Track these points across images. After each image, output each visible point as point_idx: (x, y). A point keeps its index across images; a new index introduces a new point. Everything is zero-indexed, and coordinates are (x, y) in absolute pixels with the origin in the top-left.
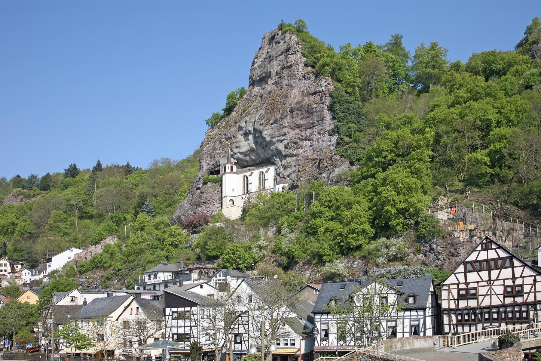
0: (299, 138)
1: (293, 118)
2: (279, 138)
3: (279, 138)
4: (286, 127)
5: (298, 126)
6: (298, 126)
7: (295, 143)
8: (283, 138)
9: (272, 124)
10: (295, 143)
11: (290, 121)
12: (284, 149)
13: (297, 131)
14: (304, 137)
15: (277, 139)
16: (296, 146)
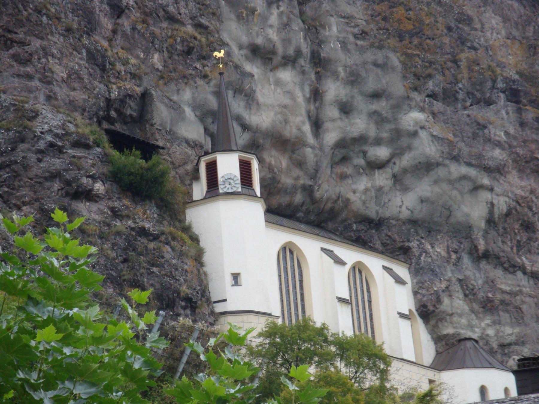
1: (522, 124)
2: (472, 172)
4: (498, 144)
9: (432, 96)
11: (512, 131)
15: (464, 170)
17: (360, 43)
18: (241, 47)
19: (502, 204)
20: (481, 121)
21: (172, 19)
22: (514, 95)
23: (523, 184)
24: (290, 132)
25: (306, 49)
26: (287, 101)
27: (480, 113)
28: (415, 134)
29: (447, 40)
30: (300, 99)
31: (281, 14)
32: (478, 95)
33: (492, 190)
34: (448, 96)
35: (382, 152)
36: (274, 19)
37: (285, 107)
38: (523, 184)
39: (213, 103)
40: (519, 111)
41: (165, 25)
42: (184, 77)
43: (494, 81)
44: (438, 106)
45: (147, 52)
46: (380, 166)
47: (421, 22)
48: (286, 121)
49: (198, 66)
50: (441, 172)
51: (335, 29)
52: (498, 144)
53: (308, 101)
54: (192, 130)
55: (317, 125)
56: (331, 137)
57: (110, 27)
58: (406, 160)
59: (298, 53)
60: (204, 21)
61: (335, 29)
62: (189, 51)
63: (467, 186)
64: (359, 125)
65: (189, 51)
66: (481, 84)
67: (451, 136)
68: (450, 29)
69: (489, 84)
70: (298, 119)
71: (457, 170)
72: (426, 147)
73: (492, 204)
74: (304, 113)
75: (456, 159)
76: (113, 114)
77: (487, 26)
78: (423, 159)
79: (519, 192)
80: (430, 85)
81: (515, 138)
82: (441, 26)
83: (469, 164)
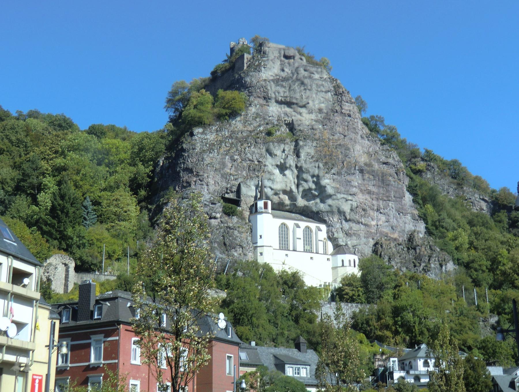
0: (370, 207)
1: (364, 180)
2: (345, 196)
3: (345, 196)
4: (355, 187)
5: (369, 193)
6: (369, 193)
7: (364, 210)
8: (350, 198)
9: (334, 174)
10: (364, 210)
11: (360, 182)
12: (349, 211)
13: (367, 197)
14: (376, 208)
15: (342, 196)
16: (363, 213)
17: (311, 160)
18: (272, 165)
19: (355, 204)
20: (349, 180)
22: (361, 171)
27: (349, 178)
30: (292, 179)
33: (351, 200)
34: (339, 174)
40: (363, 176)
41: (248, 162)
44: (335, 177)
45: (241, 171)
48: (286, 186)
50: (334, 197)
52: (355, 187)
57: (231, 165)
63: (344, 200)
67: (338, 186)
69: (353, 168)
71: (339, 196)
75: (340, 193)
76: (228, 191)
79: (362, 200)
80: (333, 171)
81: (361, 184)
83: (344, 194)
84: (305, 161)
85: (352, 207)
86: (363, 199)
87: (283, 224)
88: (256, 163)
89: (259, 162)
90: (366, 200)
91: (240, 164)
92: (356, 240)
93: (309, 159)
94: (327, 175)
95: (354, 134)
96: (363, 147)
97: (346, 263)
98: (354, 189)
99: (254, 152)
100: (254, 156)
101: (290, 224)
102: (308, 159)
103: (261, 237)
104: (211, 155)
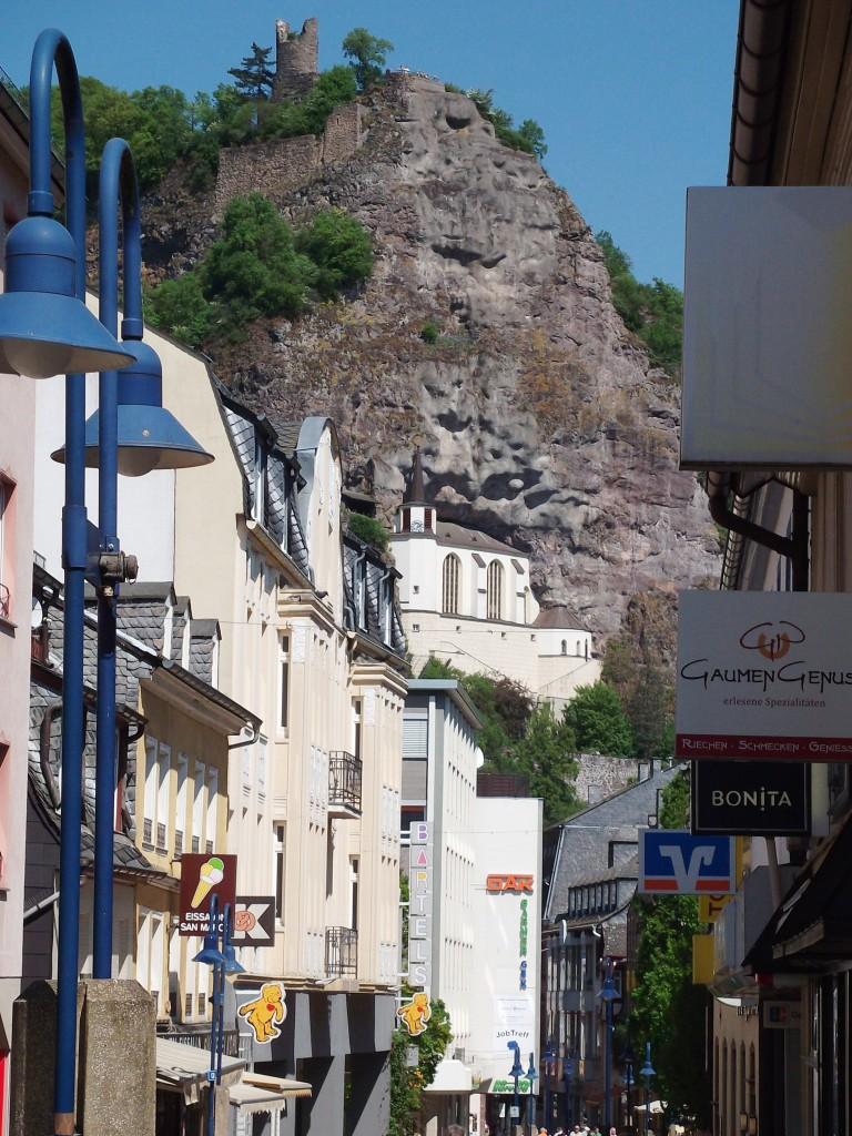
1: (615, 455)
2: (576, 494)
4: (597, 473)
9: (557, 442)
11: (607, 461)
17: (511, 407)
20: (586, 457)
21: (390, 405)
23: (610, 497)
24: (458, 471)
25: (475, 416)
26: (459, 452)
27: (584, 450)
28: (541, 473)
29: (570, 398)
30: (468, 449)
31: (461, 392)
32: (586, 437)
35: (518, 483)
36: (455, 396)
37: (458, 456)
38: (610, 497)
39: (410, 463)
40: (614, 446)
41: (386, 408)
42: (395, 447)
43: (599, 425)
45: (372, 431)
46: (518, 491)
47: (555, 385)
48: (458, 465)
49: (404, 438)
50: (555, 496)
51: (495, 399)
53: (474, 448)
54: (399, 483)
55: (477, 462)
56: (486, 473)
58: (534, 489)
59: (470, 419)
60: (411, 404)
61: (495, 399)
62: (399, 429)
64: (506, 465)
65: (399, 429)
66: (590, 429)
68: (573, 389)
70: (466, 463)
72: (547, 481)
73: (588, 514)
74: (470, 459)
77: (600, 381)
78: (543, 489)
79: (607, 504)
82: (568, 388)
84: (500, 408)
85: (586, 520)
86: (609, 500)
87: (451, 557)
88: (402, 410)
89: (407, 408)
90: (616, 503)
91: (370, 414)
92: (590, 595)
93: (509, 403)
94: (545, 446)
95: (598, 341)
96: (615, 372)
97: (571, 650)
98: (596, 477)
99: (397, 383)
100: (398, 393)
101: (465, 555)
102: (506, 404)
103: (416, 588)
104: (317, 393)
